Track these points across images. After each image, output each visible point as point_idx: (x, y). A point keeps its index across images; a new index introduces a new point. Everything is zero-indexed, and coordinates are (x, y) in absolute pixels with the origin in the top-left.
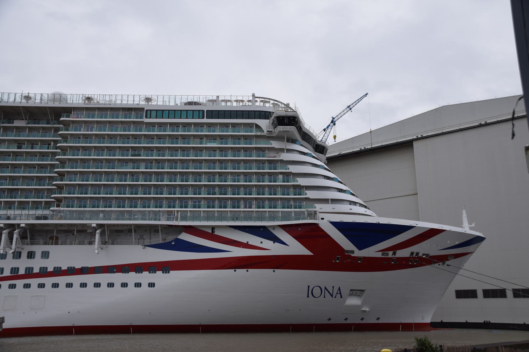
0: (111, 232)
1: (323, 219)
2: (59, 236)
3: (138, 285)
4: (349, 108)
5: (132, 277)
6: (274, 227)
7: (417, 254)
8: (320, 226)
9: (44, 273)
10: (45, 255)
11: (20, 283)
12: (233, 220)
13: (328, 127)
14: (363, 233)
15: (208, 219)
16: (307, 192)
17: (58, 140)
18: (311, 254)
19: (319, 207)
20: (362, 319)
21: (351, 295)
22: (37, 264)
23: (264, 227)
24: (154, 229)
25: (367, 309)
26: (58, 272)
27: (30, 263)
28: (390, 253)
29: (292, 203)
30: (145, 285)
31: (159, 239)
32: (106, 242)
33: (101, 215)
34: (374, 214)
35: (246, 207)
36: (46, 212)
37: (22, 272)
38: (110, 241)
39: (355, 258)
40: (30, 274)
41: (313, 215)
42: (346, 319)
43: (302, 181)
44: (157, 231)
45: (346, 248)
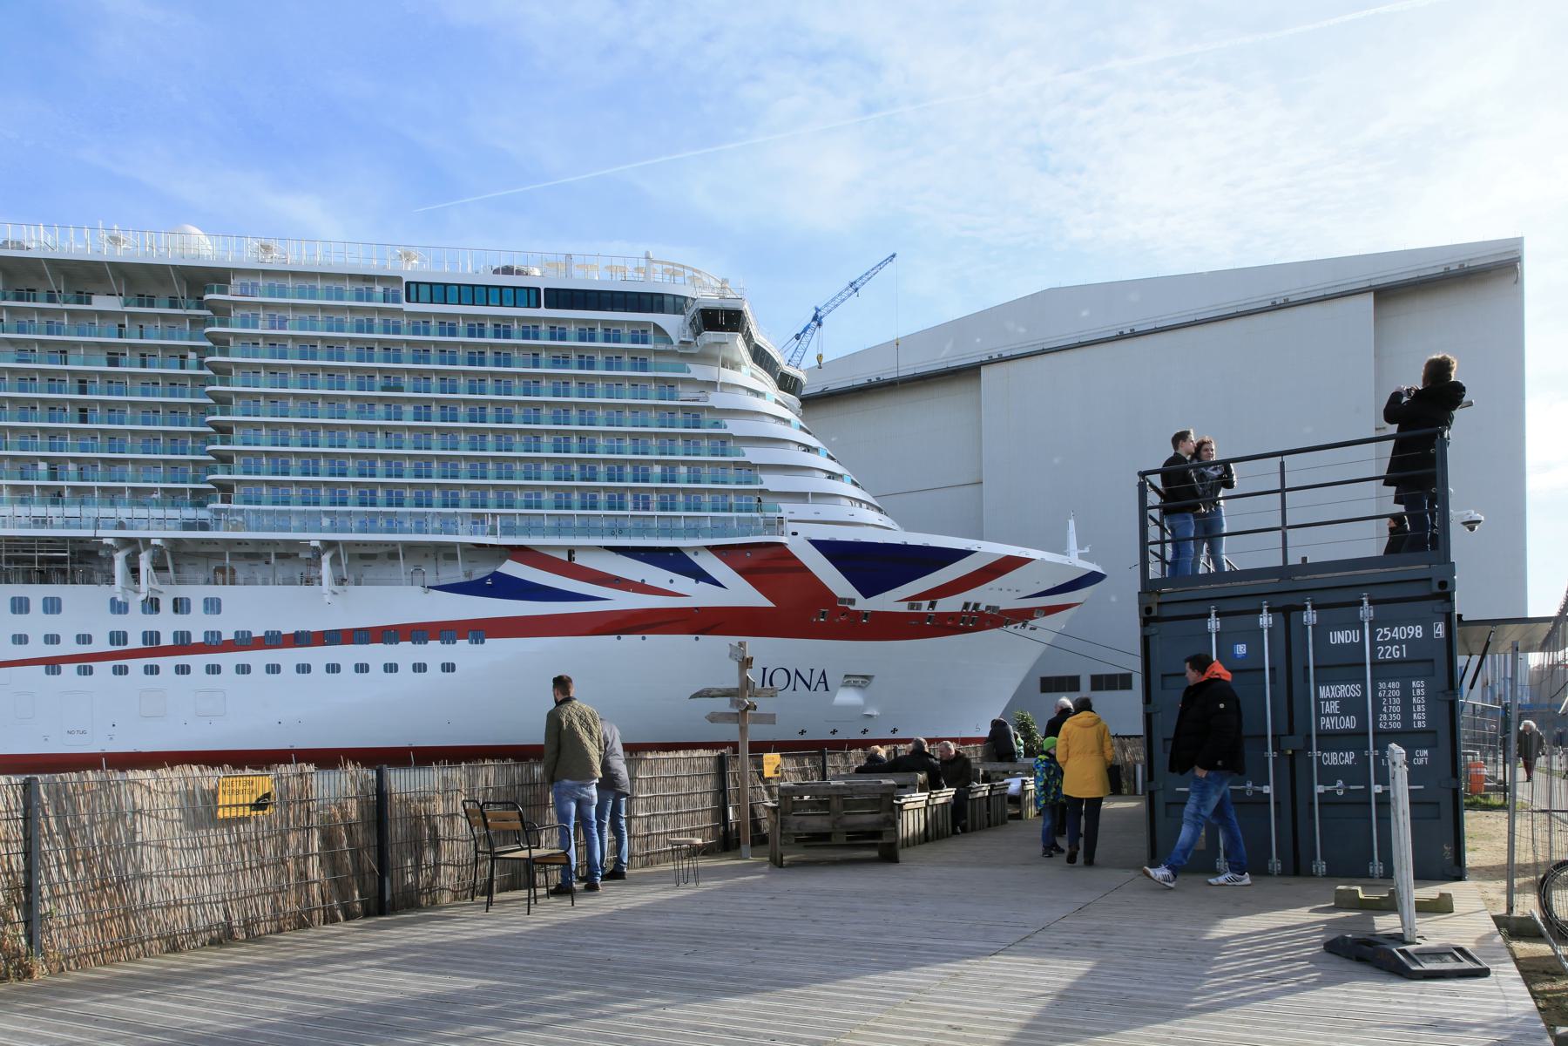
0: (351, 557)
1: (795, 534)
2: (236, 565)
4: (854, 287)
6: (696, 550)
7: (977, 605)
8: (790, 548)
10: (213, 606)
12: (613, 534)
13: (805, 331)
14: (872, 564)
15: (558, 531)
16: (763, 477)
17: (205, 348)
18: (771, 605)
19: (787, 509)
20: (865, 731)
21: (845, 685)
22: (197, 625)
23: (676, 550)
24: (446, 552)
25: (875, 713)
26: (244, 642)
27: (182, 623)
28: (925, 604)
30: (434, 668)
31: (457, 574)
32: (344, 580)
33: (326, 522)
34: (896, 527)
35: (636, 508)
36: (203, 514)
37: (167, 640)
38: (352, 578)
40: (183, 645)
42: (834, 732)
43: (753, 455)
44: (453, 557)
45: (839, 595)
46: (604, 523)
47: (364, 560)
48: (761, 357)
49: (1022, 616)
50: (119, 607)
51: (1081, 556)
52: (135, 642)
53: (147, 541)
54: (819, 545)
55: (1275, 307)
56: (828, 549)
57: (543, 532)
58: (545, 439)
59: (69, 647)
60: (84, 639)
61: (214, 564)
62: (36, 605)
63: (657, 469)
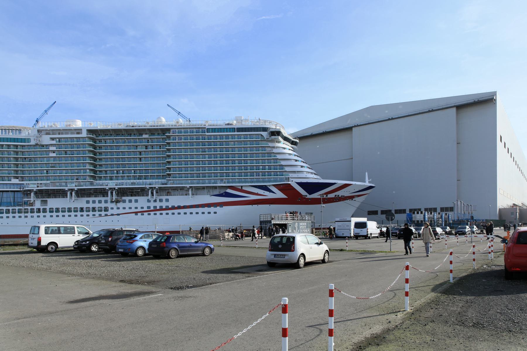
3: (209, 213)
5: (206, 210)
6: (270, 186)
9: (167, 208)
10: (167, 200)
11: (158, 213)
15: (239, 182)
18: (286, 197)
19: (291, 175)
22: (164, 204)
24: (215, 187)
26: (173, 208)
29: (278, 173)
31: (217, 192)
37: (158, 208)
39: (308, 198)
40: (161, 209)
41: (288, 179)
43: (283, 163)
46: (249, 180)
47: (197, 190)
48: (286, 139)
49: (351, 198)
50: (149, 201)
51: (369, 182)
52: (152, 208)
53: (155, 187)
54: (298, 183)
55: (429, 111)
56: (300, 184)
57: (235, 182)
58: (236, 161)
59: (139, 210)
60: (142, 208)
61: (167, 191)
62: (133, 201)
63: (261, 167)
